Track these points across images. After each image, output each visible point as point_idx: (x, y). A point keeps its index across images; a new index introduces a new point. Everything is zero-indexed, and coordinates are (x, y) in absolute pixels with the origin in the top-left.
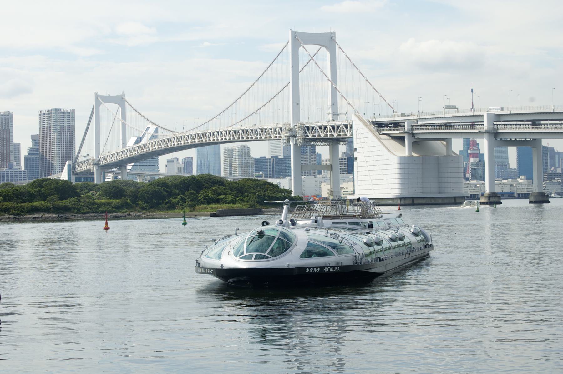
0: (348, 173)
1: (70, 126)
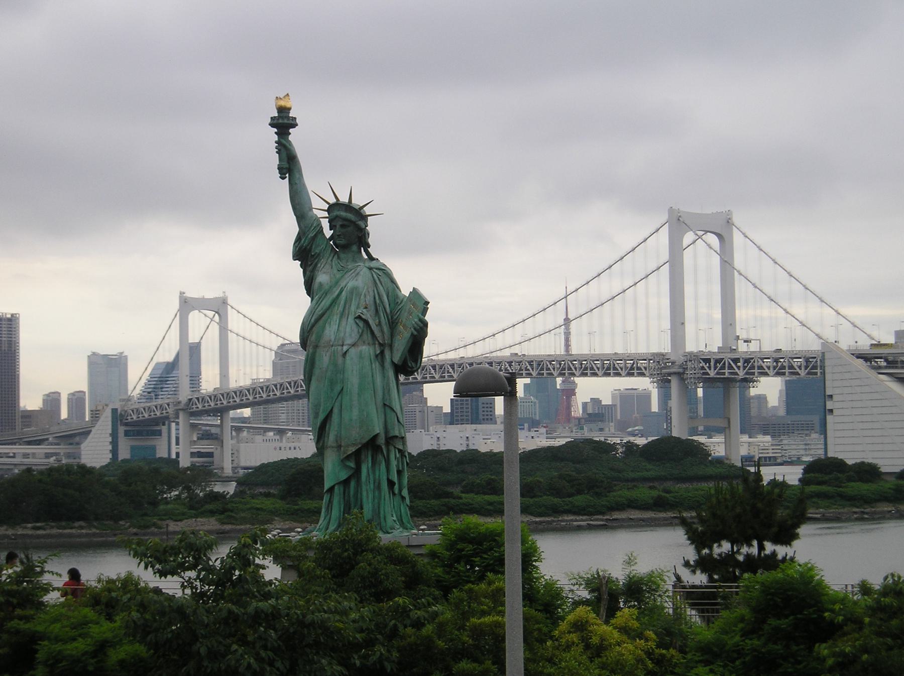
1: (10, 341)
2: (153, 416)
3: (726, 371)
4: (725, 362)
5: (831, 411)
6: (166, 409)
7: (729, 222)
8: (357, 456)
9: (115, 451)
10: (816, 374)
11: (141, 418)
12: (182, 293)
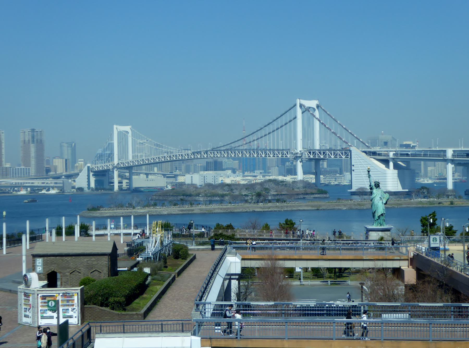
0: (214, 171)
2: (103, 169)
3: (317, 156)
4: (316, 153)
5: (353, 170)
6: (109, 167)
8: (380, 216)
10: (348, 157)
11: (99, 170)
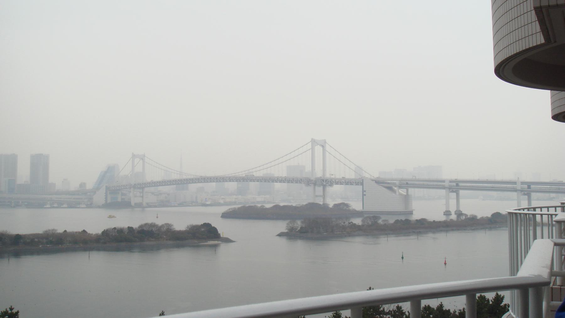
5: (365, 195)
7: (325, 142)
9: (106, 198)
12: (133, 153)
